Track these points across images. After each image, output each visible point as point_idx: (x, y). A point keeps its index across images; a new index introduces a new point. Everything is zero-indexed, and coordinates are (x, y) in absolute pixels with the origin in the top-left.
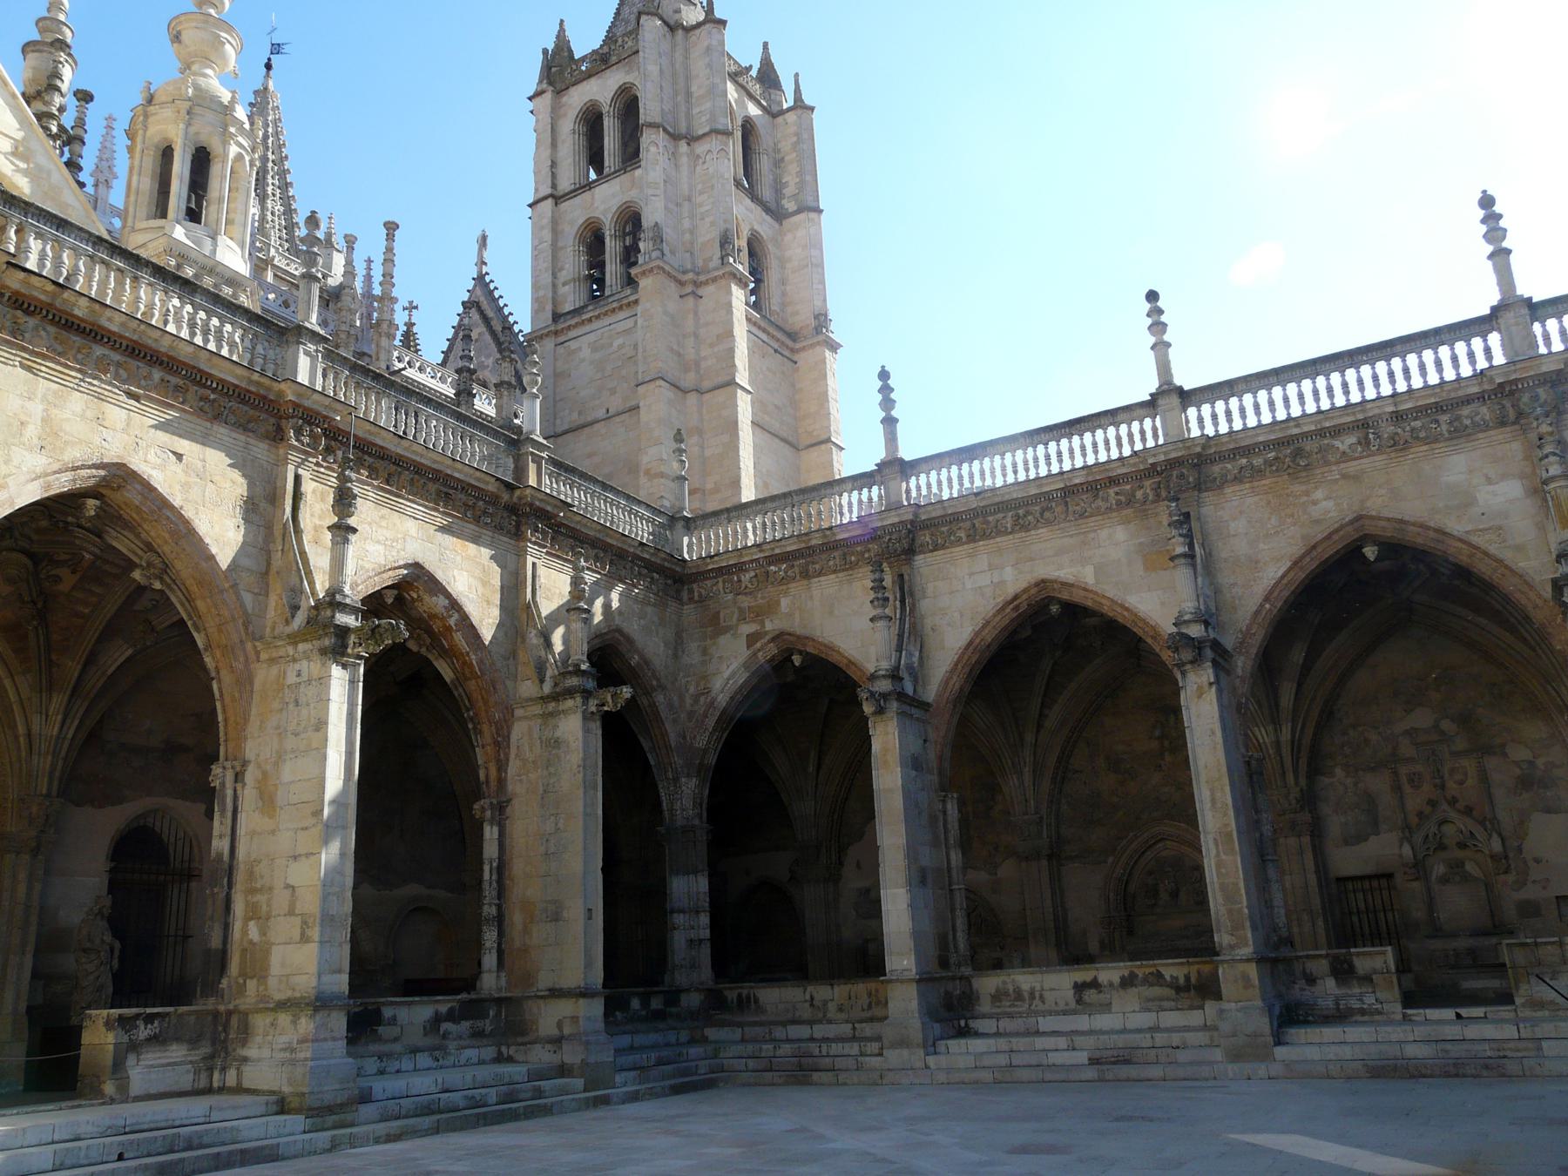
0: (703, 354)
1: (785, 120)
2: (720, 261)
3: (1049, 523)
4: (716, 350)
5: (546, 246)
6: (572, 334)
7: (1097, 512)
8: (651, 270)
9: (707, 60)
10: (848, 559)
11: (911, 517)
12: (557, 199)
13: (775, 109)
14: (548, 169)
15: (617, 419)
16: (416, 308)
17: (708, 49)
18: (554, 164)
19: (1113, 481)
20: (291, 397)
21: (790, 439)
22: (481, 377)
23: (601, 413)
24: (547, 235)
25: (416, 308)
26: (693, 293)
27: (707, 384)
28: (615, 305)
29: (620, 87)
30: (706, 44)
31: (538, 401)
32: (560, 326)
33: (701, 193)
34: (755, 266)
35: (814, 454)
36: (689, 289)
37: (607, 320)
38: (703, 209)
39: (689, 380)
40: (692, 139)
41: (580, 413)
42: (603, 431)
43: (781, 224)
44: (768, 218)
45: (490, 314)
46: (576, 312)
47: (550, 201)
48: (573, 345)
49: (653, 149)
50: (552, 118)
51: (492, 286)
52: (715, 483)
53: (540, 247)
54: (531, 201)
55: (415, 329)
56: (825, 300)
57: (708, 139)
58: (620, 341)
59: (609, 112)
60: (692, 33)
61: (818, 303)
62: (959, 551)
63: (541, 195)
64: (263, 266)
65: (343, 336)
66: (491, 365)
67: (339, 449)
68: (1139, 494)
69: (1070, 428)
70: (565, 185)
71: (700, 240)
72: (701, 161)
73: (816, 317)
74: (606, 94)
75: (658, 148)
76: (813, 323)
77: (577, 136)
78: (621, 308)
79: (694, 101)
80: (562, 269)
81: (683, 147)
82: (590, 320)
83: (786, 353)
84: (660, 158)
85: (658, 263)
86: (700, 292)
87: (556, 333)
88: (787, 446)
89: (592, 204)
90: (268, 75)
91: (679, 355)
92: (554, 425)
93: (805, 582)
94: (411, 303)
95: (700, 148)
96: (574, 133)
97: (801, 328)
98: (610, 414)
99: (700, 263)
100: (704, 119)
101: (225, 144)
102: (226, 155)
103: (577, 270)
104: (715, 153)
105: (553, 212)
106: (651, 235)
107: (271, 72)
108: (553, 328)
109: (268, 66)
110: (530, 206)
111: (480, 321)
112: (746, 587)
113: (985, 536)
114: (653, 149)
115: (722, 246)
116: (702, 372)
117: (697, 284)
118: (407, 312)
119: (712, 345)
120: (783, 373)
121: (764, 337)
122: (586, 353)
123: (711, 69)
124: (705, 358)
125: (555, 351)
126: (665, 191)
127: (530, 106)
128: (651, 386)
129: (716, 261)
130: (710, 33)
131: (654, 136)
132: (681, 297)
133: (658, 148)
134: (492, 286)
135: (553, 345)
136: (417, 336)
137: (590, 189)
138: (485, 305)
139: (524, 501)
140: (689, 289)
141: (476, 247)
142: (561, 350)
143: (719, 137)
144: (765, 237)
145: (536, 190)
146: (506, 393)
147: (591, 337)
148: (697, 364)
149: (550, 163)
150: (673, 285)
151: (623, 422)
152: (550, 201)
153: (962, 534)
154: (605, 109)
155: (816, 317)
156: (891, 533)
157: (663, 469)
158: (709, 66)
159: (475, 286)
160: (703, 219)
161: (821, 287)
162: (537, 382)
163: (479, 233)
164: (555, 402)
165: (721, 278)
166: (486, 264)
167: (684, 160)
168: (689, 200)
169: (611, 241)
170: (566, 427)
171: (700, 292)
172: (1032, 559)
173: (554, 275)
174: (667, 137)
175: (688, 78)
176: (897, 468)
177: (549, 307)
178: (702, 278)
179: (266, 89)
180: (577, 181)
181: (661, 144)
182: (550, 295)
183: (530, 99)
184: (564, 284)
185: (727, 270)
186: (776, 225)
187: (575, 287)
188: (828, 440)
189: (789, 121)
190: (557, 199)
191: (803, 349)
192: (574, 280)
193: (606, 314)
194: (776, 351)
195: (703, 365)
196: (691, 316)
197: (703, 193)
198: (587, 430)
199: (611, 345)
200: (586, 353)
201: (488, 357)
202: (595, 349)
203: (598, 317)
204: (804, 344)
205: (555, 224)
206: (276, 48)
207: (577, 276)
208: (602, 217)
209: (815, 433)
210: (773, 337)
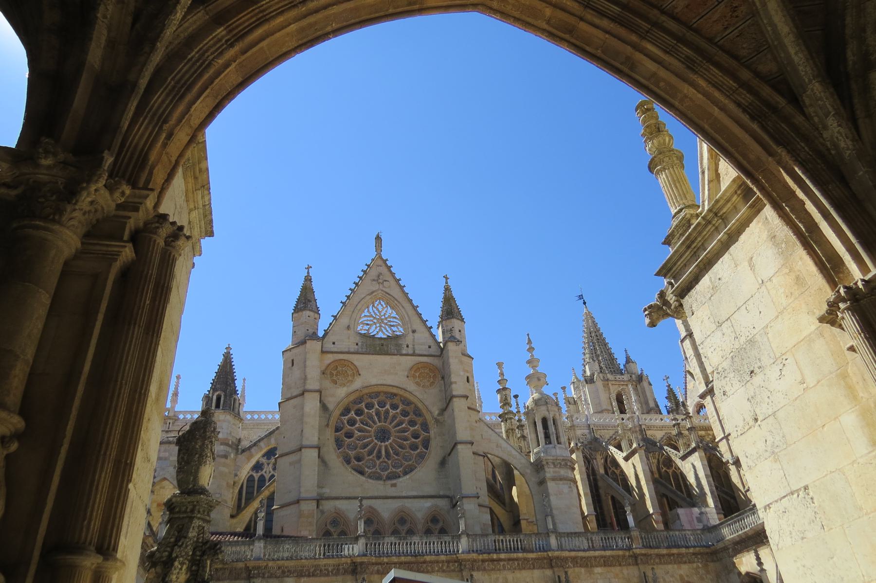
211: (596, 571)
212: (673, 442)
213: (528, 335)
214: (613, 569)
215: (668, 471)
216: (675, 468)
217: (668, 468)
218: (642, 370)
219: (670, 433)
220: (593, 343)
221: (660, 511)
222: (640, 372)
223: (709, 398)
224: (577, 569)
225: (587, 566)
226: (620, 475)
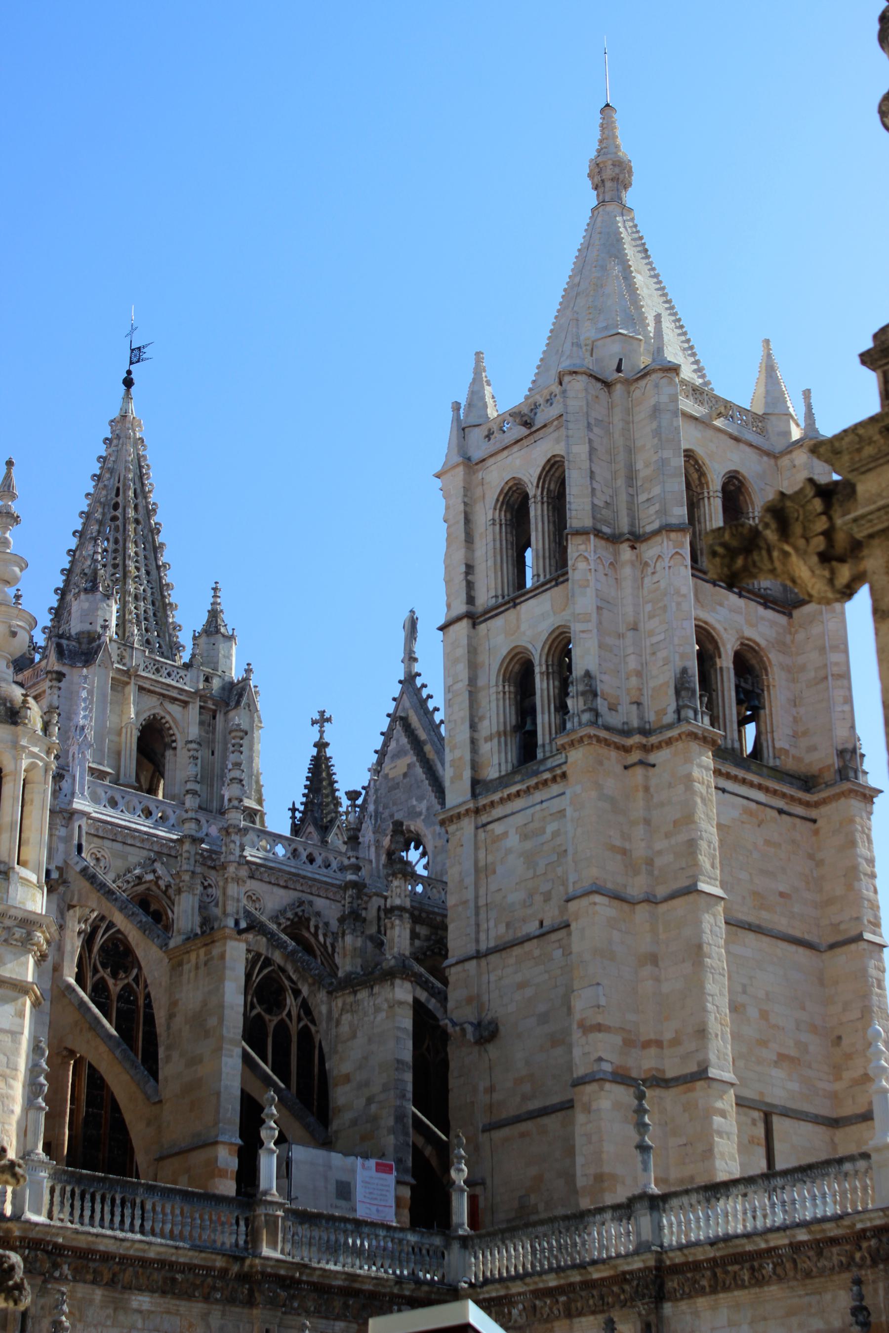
0: (658, 846)
1: (792, 461)
2: (676, 716)
3: (780, 1279)
4: (673, 841)
5: (462, 685)
6: (498, 812)
7: (822, 1272)
8: (581, 740)
9: (654, 425)
10: (606, 1300)
11: (652, 1263)
12: (474, 618)
13: (779, 445)
14: (462, 577)
15: (554, 937)
16: (329, 720)
17: (656, 411)
18: (469, 569)
19: (834, 1241)
20: (17, 1233)
21: (807, 937)
22: (412, 828)
23: (532, 928)
24: (463, 671)
25: (329, 720)
26: (641, 763)
27: (661, 891)
28: (547, 775)
29: (549, 461)
30: (653, 401)
31: (275, 1155)
32: (483, 801)
33: (651, 617)
34: (748, 687)
35: (842, 957)
36: (635, 756)
37: (538, 796)
38: (654, 640)
39: (636, 887)
40: (636, 539)
41: (508, 925)
42: (537, 953)
43: (790, 616)
44: (769, 614)
45: (423, 735)
46: (503, 781)
47: (464, 624)
48: (498, 828)
49: (582, 565)
50: (465, 504)
51: (425, 693)
52: (676, 1032)
53: (455, 687)
54: (441, 621)
55: (329, 752)
56: (853, 727)
57: (658, 539)
58: (551, 828)
59: (535, 496)
60: (635, 385)
61: (841, 733)
62: (702, 1302)
63: (455, 613)
64: (127, 679)
65: (186, 877)
66: (424, 811)
67: (65, 1263)
68: (858, 1256)
69: (802, 1172)
70: (484, 598)
71: (652, 684)
72: (650, 570)
73: (841, 753)
74: (531, 472)
75: (589, 564)
76: (836, 763)
77: (498, 527)
78: (554, 779)
79: (639, 484)
80: (482, 718)
81: (626, 552)
82: (518, 794)
83: (799, 810)
84: (591, 577)
85: (592, 731)
86: (652, 758)
87: (477, 811)
88: (801, 950)
89: (518, 627)
90: (128, 396)
91: (624, 852)
92: (477, 941)
93: (567, 1322)
94: (322, 713)
95: (650, 551)
96: (494, 524)
97: (820, 770)
98: (544, 930)
99: (651, 717)
100: (652, 510)
101: (17, 759)
102: (16, 772)
103: (502, 720)
104: (667, 560)
105: (469, 638)
106: (581, 688)
107: (133, 389)
108: (471, 805)
109: (128, 383)
110: (441, 629)
111: (408, 747)
112: (516, 1321)
113: (726, 1289)
114: (582, 565)
115: (678, 693)
116: (656, 872)
117: (647, 749)
118: (317, 727)
119: (667, 836)
120: (793, 842)
121: (760, 796)
122: (513, 841)
123: (660, 439)
124: (660, 853)
125: (476, 836)
126: (600, 623)
127: (438, 483)
128: (584, 902)
129: (670, 717)
130: (657, 386)
131: (582, 547)
132: (626, 768)
133: (589, 564)
134: (425, 693)
135: (472, 827)
136: (333, 762)
137: (515, 606)
138: (415, 721)
139: (254, 1270)
140: (635, 756)
141: (401, 635)
142: (482, 834)
143: (673, 535)
144: (763, 643)
145: (449, 606)
146: (397, 922)
147: (519, 819)
148: (650, 862)
149: (463, 569)
150: (613, 754)
151: (559, 940)
152: (464, 624)
153: (704, 1283)
154: (531, 491)
155: (841, 753)
156: (639, 1278)
157: (600, 1019)
158: (657, 433)
159: (402, 693)
160: (654, 654)
161: (846, 708)
162: (273, 1137)
163: (407, 614)
164: (477, 908)
165: (677, 740)
166: (416, 660)
167: (627, 571)
168: (635, 628)
169: (542, 681)
170: (492, 944)
171: (652, 758)
172: (765, 1319)
173: (473, 727)
174: (603, 543)
175: (630, 451)
176: (646, 1203)
177: (467, 774)
178: (654, 740)
179: (124, 417)
180: (500, 592)
181: (592, 557)
182: (468, 757)
183: (438, 476)
184: (489, 738)
185: (683, 729)
186: (782, 620)
187: (499, 742)
188: (859, 938)
189: (797, 463)
190: (474, 618)
191: (824, 802)
192: (499, 734)
193: (536, 787)
194: (781, 812)
195: (659, 862)
196: (641, 794)
197: (654, 616)
198: (517, 951)
199: (543, 831)
200: (513, 841)
201: (420, 799)
202: (525, 837)
203: (528, 791)
204: (823, 795)
205: (473, 651)
206: (136, 355)
207: (502, 728)
208: (530, 647)
209: (842, 927)
210: (775, 792)
211: (135, 1304)
212: (307, 935)
213: (10, 463)
214: (183, 1306)
215: (267, 1017)
216: (289, 1014)
217: (269, 1011)
218: (248, 671)
219: (311, 903)
220: (117, 529)
221: (239, 1141)
222: (236, 674)
223: (467, 825)
224: (82, 1290)
225: (112, 1283)
226: (120, 997)
